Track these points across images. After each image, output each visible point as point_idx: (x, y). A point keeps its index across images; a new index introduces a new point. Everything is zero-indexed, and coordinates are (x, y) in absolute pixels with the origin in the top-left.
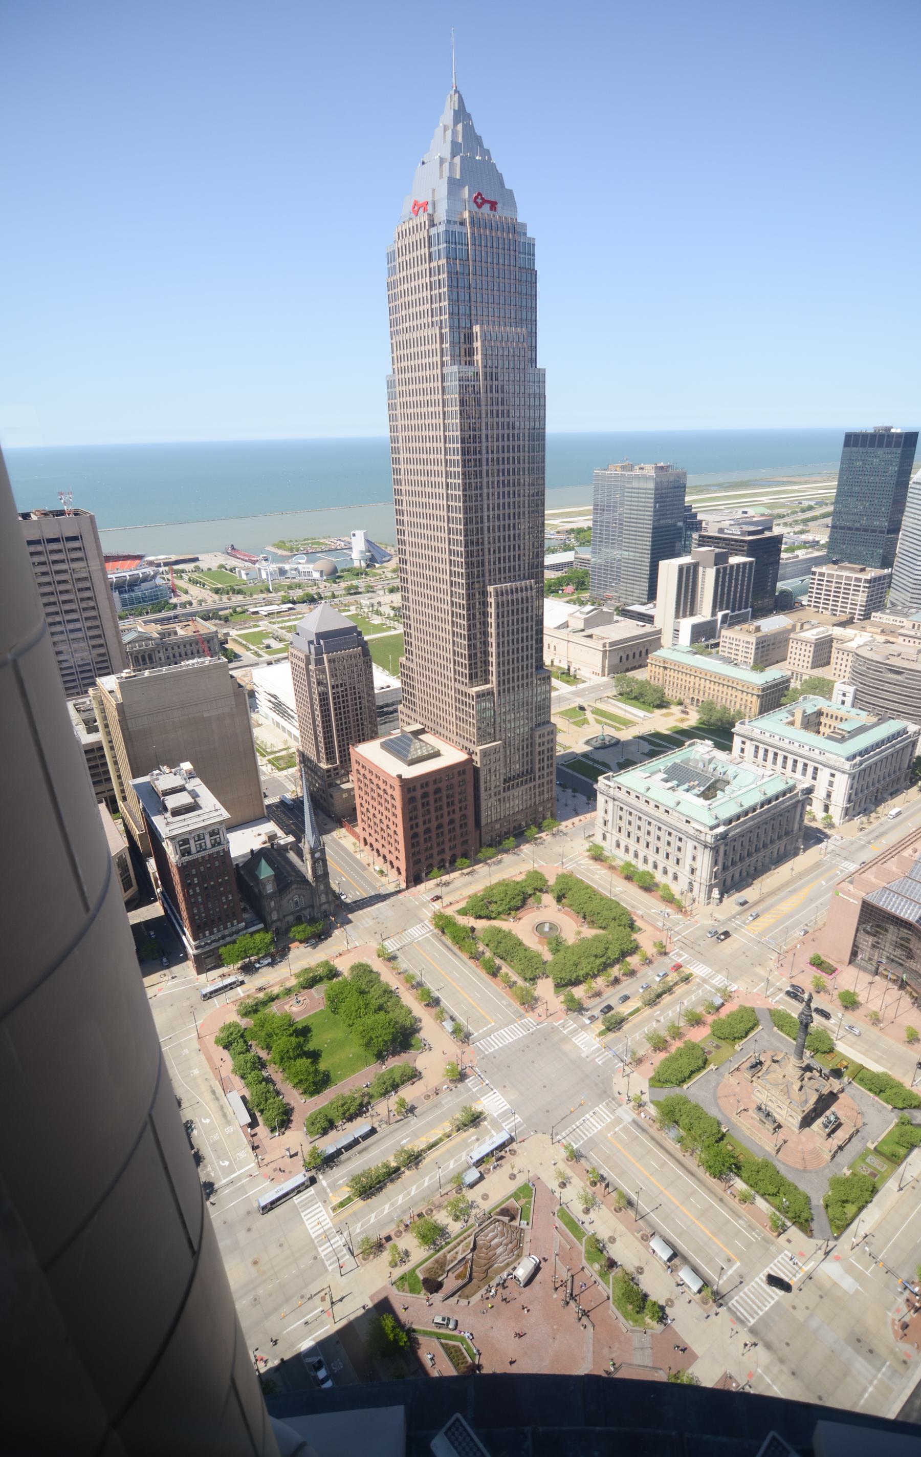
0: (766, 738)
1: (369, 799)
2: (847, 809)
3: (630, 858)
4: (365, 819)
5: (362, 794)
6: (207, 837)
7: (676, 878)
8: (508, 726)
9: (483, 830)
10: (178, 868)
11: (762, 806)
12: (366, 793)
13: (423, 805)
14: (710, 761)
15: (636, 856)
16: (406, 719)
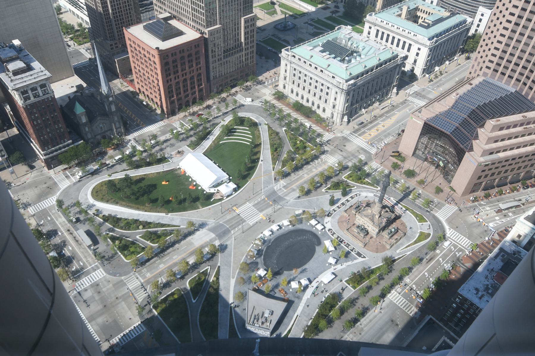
0: (384, 24)
1: (140, 64)
2: (424, 69)
3: (299, 99)
4: (138, 76)
5: (135, 60)
6: (39, 89)
7: (324, 110)
8: (225, 15)
9: (212, 83)
10: (24, 108)
11: (377, 68)
12: (137, 60)
13: (174, 67)
14: (349, 39)
15: (302, 98)
16: (159, 9)
